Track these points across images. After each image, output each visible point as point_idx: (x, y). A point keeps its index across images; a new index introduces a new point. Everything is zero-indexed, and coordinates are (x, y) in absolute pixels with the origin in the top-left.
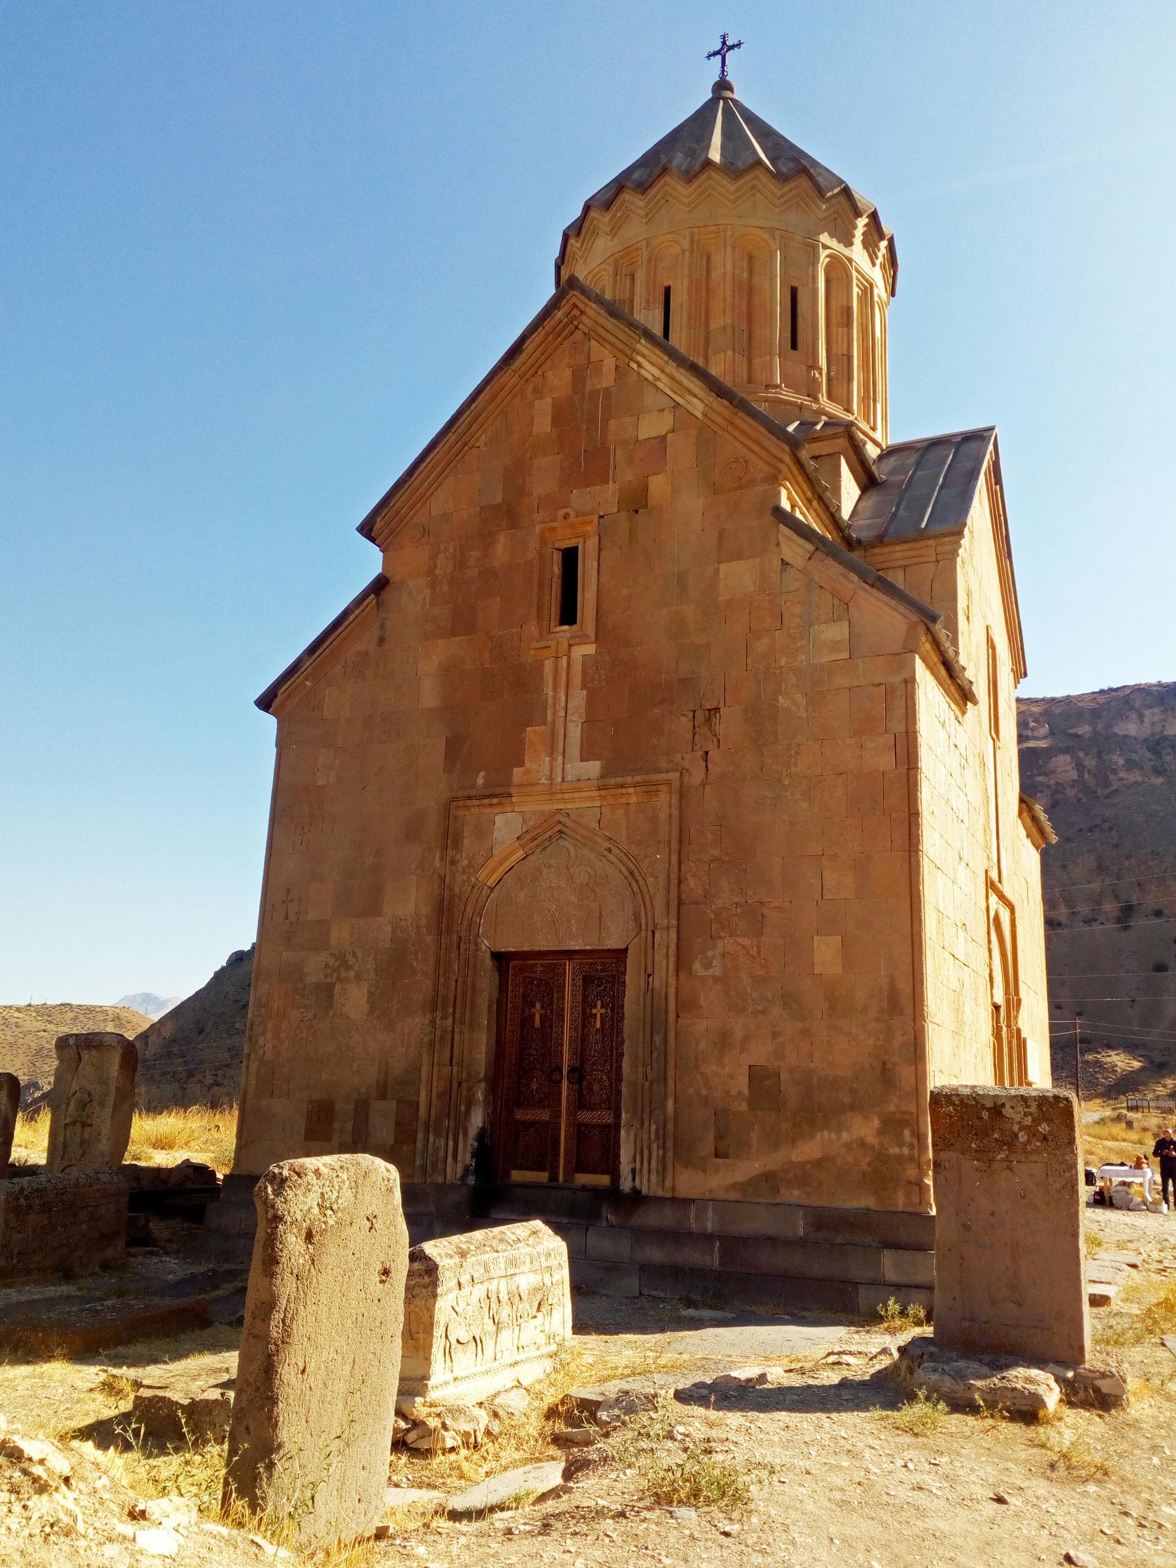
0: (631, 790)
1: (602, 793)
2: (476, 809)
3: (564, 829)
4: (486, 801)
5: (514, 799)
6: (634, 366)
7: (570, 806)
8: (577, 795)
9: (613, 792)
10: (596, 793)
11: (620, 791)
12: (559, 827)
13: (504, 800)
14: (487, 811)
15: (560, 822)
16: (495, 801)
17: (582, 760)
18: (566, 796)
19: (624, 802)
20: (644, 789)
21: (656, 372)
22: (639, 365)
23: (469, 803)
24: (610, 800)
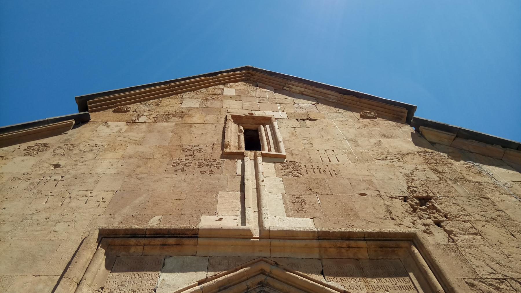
0: (362, 243)
1: (325, 243)
2: (140, 249)
3: (270, 280)
4: (159, 241)
5: (200, 241)
6: (288, 89)
7: (278, 255)
8: (289, 243)
9: (338, 243)
10: (315, 243)
11: (345, 243)
12: (261, 278)
13: (186, 241)
14: (156, 252)
15: (263, 272)
16: (172, 241)
17: (288, 216)
18: (275, 242)
19: (351, 255)
20: (379, 243)
21: (302, 89)
22: (290, 88)
23: (133, 241)
24: (333, 251)
